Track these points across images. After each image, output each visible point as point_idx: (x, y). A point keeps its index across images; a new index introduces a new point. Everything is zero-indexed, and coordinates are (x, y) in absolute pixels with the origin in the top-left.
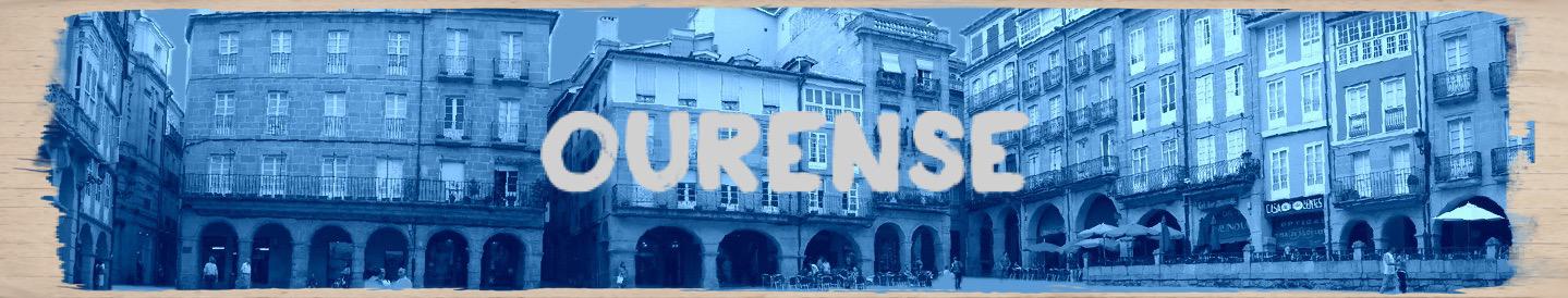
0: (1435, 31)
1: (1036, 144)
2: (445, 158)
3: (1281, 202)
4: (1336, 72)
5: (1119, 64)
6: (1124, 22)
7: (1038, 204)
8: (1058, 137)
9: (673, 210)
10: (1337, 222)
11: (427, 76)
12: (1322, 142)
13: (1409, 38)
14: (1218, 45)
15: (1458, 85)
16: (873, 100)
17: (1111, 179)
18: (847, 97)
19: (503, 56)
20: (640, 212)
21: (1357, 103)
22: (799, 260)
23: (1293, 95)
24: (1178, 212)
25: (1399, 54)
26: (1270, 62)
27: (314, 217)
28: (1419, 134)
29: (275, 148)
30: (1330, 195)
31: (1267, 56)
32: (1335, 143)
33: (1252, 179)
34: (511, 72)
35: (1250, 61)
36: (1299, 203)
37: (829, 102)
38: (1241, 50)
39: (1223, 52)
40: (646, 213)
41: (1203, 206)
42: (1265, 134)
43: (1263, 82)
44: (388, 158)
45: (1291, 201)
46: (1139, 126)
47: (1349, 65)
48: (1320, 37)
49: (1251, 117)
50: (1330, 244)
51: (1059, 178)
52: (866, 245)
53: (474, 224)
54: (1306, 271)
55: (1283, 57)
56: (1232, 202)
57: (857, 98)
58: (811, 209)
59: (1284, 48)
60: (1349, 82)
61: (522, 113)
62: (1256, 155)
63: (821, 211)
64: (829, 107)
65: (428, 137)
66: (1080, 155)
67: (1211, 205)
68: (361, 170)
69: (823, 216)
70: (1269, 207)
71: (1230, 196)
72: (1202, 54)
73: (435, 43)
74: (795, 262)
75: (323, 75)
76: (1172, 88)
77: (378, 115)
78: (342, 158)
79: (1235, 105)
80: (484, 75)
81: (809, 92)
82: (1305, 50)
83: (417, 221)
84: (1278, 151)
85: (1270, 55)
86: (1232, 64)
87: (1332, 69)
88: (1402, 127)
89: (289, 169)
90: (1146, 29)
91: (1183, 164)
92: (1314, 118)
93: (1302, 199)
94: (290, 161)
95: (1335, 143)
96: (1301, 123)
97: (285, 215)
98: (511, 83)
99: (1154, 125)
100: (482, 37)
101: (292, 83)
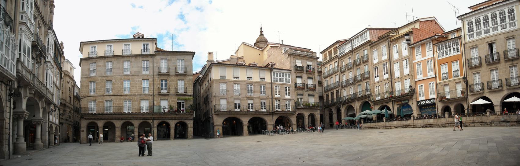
0: (467, 46)
1: (346, 86)
2: (162, 99)
3: (422, 101)
5: (370, 60)
6: (371, 47)
7: (347, 105)
8: (352, 84)
9: (233, 112)
10: (440, 106)
11: (155, 74)
12: (434, 82)
13: (460, 48)
14: (400, 53)
15: (475, 62)
16: (294, 75)
17: (369, 96)
18: (286, 74)
19: (178, 67)
20: (223, 113)
21: (444, 69)
22: (273, 125)
23: (424, 68)
24: (390, 105)
25: (457, 54)
26: (417, 57)
27: (122, 119)
28: (464, 78)
29: (108, 98)
31: (416, 56)
32: (438, 82)
33: (412, 95)
34: (181, 71)
35: (410, 58)
37: (280, 76)
39: (402, 55)
40: (225, 113)
41: (398, 103)
42: (416, 80)
43: (415, 64)
44: (144, 99)
45: (425, 100)
46: (377, 79)
47: (442, 58)
48: (432, 49)
49: (412, 75)
50: (438, 113)
51: (353, 96)
52: (294, 120)
53: (172, 119)
54: (431, 122)
55: (421, 56)
56: (407, 101)
57: (289, 75)
58: (276, 110)
59: (421, 53)
60: (442, 63)
61: (185, 84)
62: (414, 87)
63: (279, 110)
64: (280, 78)
65: (156, 93)
66: (359, 89)
67: (400, 103)
68: (136, 103)
69: (280, 112)
71: (406, 100)
72: (396, 56)
73: (157, 63)
74: (272, 126)
75: (123, 75)
76: (386, 67)
77: (140, 86)
78: (130, 100)
79: (406, 71)
80: (172, 72)
81: (274, 73)
82: (427, 54)
83: (153, 119)
84: (421, 85)
85: (417, 56)
86: (406, 59)
87: (436, 59)
89: (113, 104)
91: (391, 90)
92: (431, 74)
93: (429, 100)
94: (114, 102)
95: (438, 82)
96: (427, 76)
97: (112, 119)
98: (181, 75)
99: (381, 79)
100: (172, 61)
101: (113, 78)
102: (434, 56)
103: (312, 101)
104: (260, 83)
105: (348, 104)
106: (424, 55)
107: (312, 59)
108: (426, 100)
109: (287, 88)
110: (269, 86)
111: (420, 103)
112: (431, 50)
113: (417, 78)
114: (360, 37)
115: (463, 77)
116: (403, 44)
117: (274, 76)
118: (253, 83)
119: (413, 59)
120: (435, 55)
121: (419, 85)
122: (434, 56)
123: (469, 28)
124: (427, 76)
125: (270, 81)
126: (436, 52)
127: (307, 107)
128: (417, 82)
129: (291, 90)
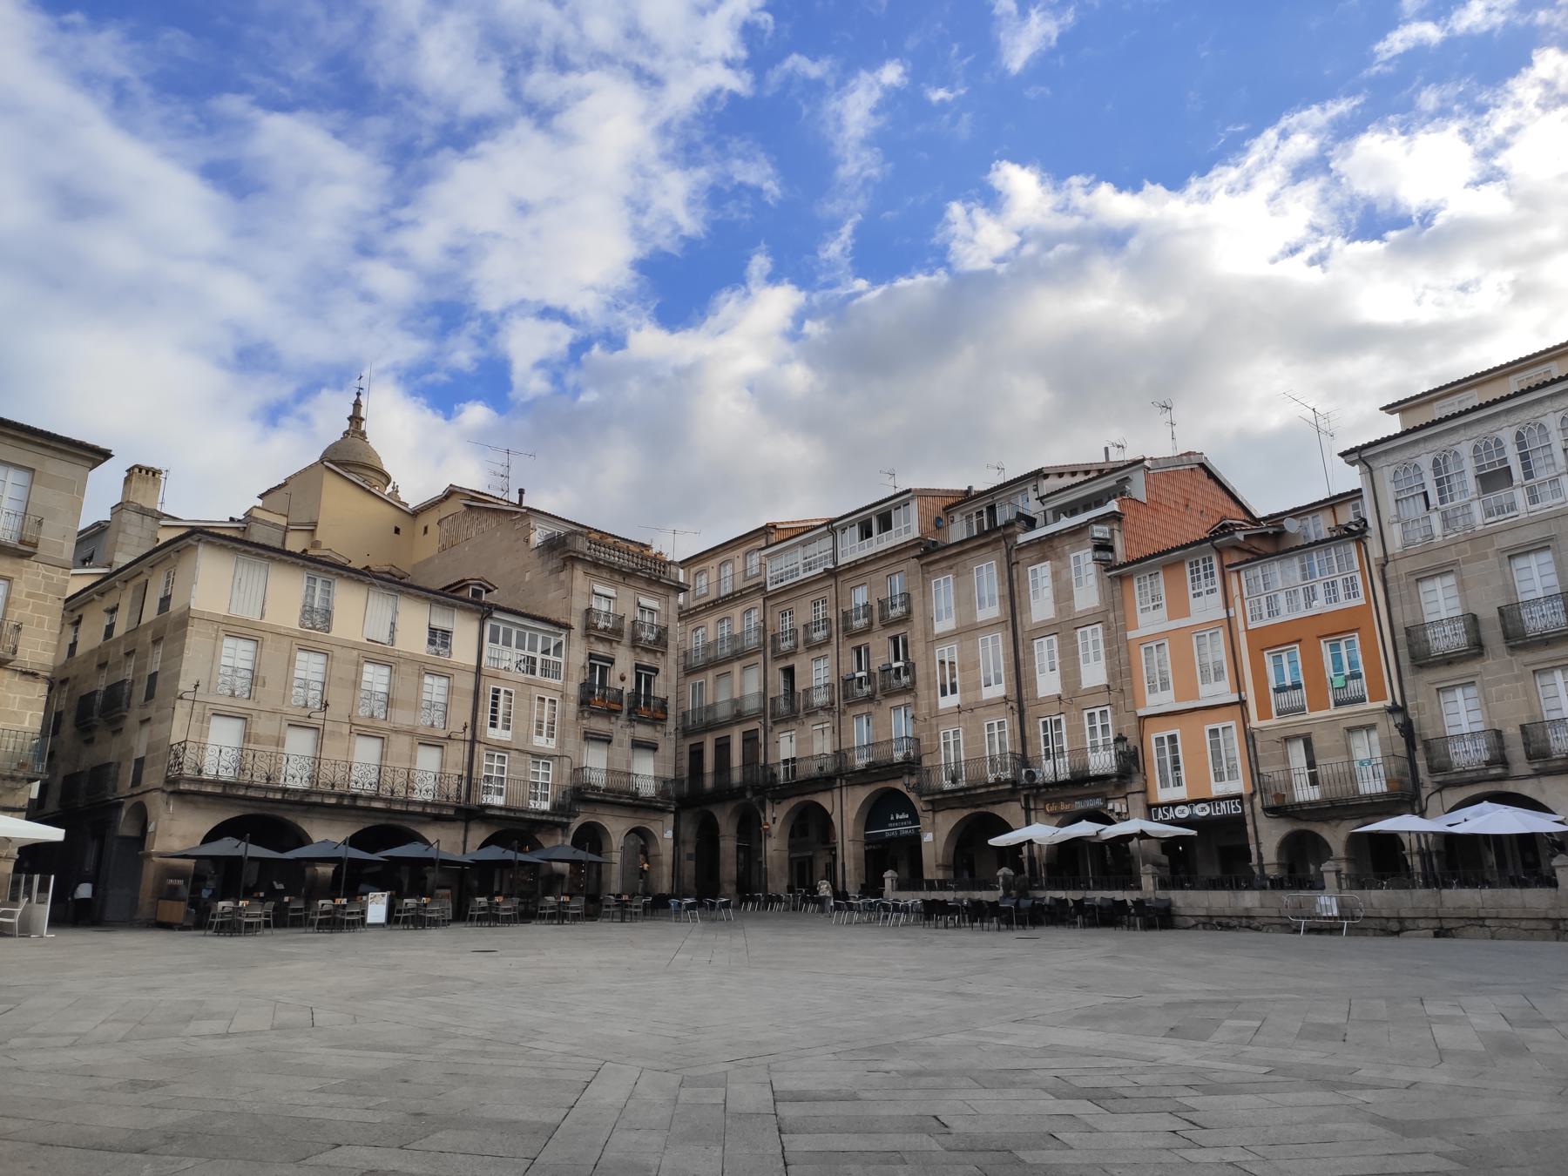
3: (1175, 804)
4: (1247, 630)
7: (794, 802)
10: (1268, 839)
12: (1232, 723)
17: (911, 766)
21: (1287, 667)
23: (1183, 662)
25: (1344, 603)
26: (1142, 618)
28: (1393, 710)
30: (1253, 795)
31: (1191, 596)
32: (1255, 723)
35: (1114, 618)
38: (1097, 604)
41: (1053, 808)
42: (1141, 712)
46: (948, 702)
48: (1218, 585)
49: (1121, 683)
50: (1261, 866)
54: (1249, 905)
55: (1163, 612)
59: (1164, 601)
62: (1133, 741)
66: (860, 733)
70: (1156, 812)
71: (1095, 796)
72: (1041, 608)
79: (1094, 673)
81: (495, 631)
82: (1194, 604)
84: (1165, 734)
87: (1241, 626)
88: (1363, 700)
90: (957, 575)
91: (1019, 750)
96: (1197, 698)
99: (971, 697)
102: (1228, 612)
103: (646, 773)
104: (427, 666)
105: (801, 799)
106: (1178, 608)
108: (1197, 802)
109: (543, 699)
110: (467, 682)
112: (1212, 591)
113: (1144, 705)
115: (1389, 703)
116: (1084, 559)
117: (494, 640)
118: (392, 659)
119: (1126, 622)
120: (1237, 610)
121: (1154, 736)
122: (1228, 612)
124: (1197, 698)
125: (474, 663)
127: (624, 799)
128: (1147, 722)
129: (564, 713)
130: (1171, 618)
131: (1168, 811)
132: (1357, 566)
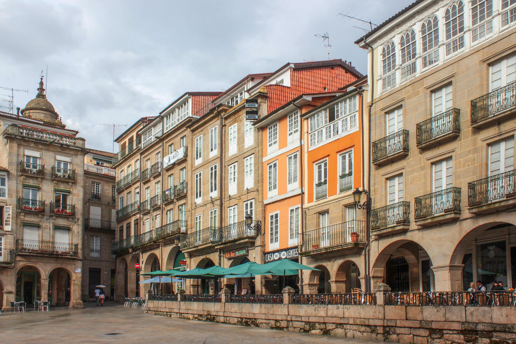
0: (377, 108)
3: (274, 252)
4: (308, 152)
5: (189, 159)
14: (241, 140)
24: (214, 257)
26: (269, 149)
32: (306, 205)
36: (284, 252)
39: (243, 147)
42: (266, 202)
43: (265, 165)
45: (279, 251)
46: (199, 201)
48: (299, 128)
59: (277, 139)
67: (232, 255)
76: (216, 172)
79: (249, 182)
82: (290, 139)
84: (274, 214)
85: (270, 145)
86: (251, 152)
92: (294, 188)
93: (287, 250)
96: (286, 192)
102: (301, 142)
107: (73, 152)
111: (270, 259)
113: (266, 198)
114: (177, 110)
120: (305, 142)
121: (271, 214)
122: (301, 142)
123: (384, 61)
126: (306, 135)
128: (268, 206)
130: (280, 148)
131: (271, 256)
132: (357, 109)
